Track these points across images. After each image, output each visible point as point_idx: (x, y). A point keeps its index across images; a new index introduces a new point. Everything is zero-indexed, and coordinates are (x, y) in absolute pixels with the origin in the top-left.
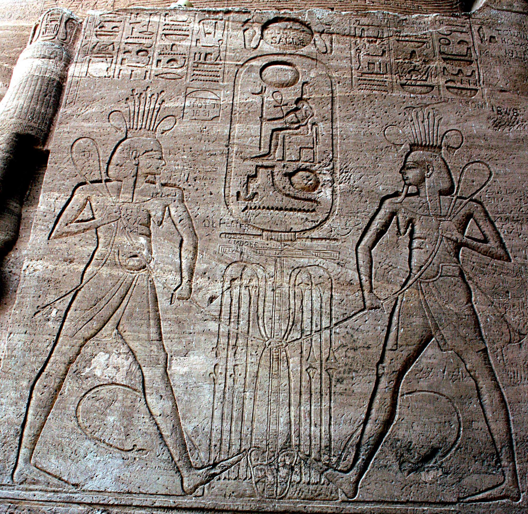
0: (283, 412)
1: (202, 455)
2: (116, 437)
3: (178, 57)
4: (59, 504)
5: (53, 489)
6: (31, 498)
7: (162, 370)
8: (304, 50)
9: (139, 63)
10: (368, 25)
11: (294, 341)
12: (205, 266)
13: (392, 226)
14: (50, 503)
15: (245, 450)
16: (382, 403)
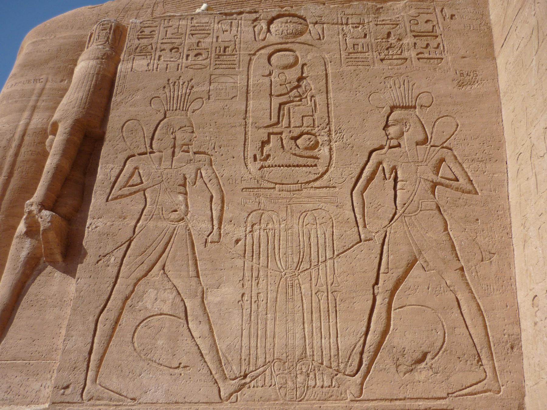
0: (299, 329)
1: (234, 368)
2: (165, 357)
5: (115, 403)
7: (200, 300)
8: (302, 39)
10: (352, 15)
11: (305, 270)
12: (231, 215)
13: (379, 173)
15: (269, 362)
16: (379, 317)
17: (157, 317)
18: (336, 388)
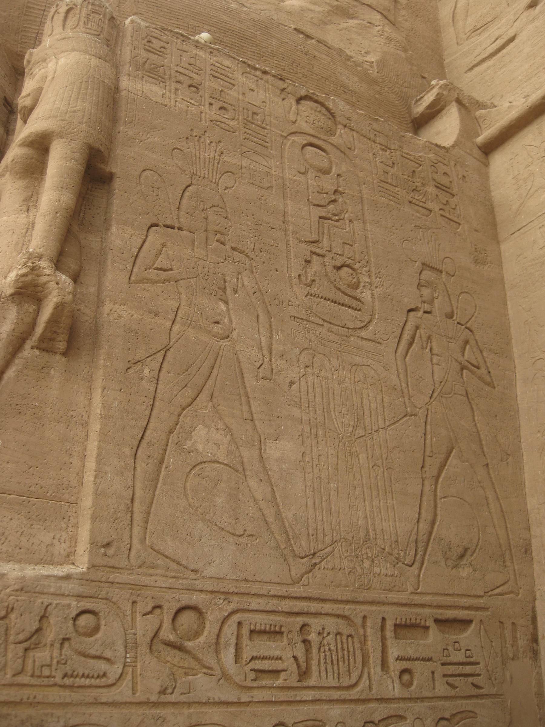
2: (226, 520)
3: (229, 107)
4: (182, 591)
5: (173, 574)
6: (153, 584)
7: (258, 452)
9: (192, 99)
11: (360, 437)
14: (173, 590)
15: (336, 541)
17: (210, 464)
18: (398, 578)
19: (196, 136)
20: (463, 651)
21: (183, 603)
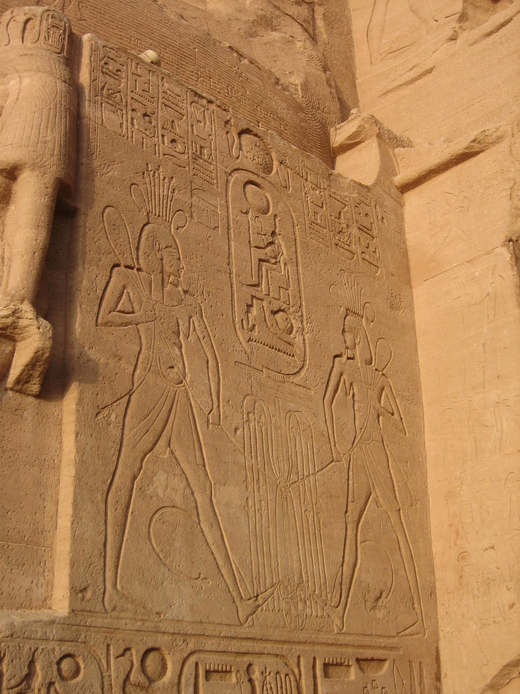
4: (147, 634)
14: (140, 633)
17: (169, 509)
19: (151, 171)
20: (380, 688)
21: (150, 645)
